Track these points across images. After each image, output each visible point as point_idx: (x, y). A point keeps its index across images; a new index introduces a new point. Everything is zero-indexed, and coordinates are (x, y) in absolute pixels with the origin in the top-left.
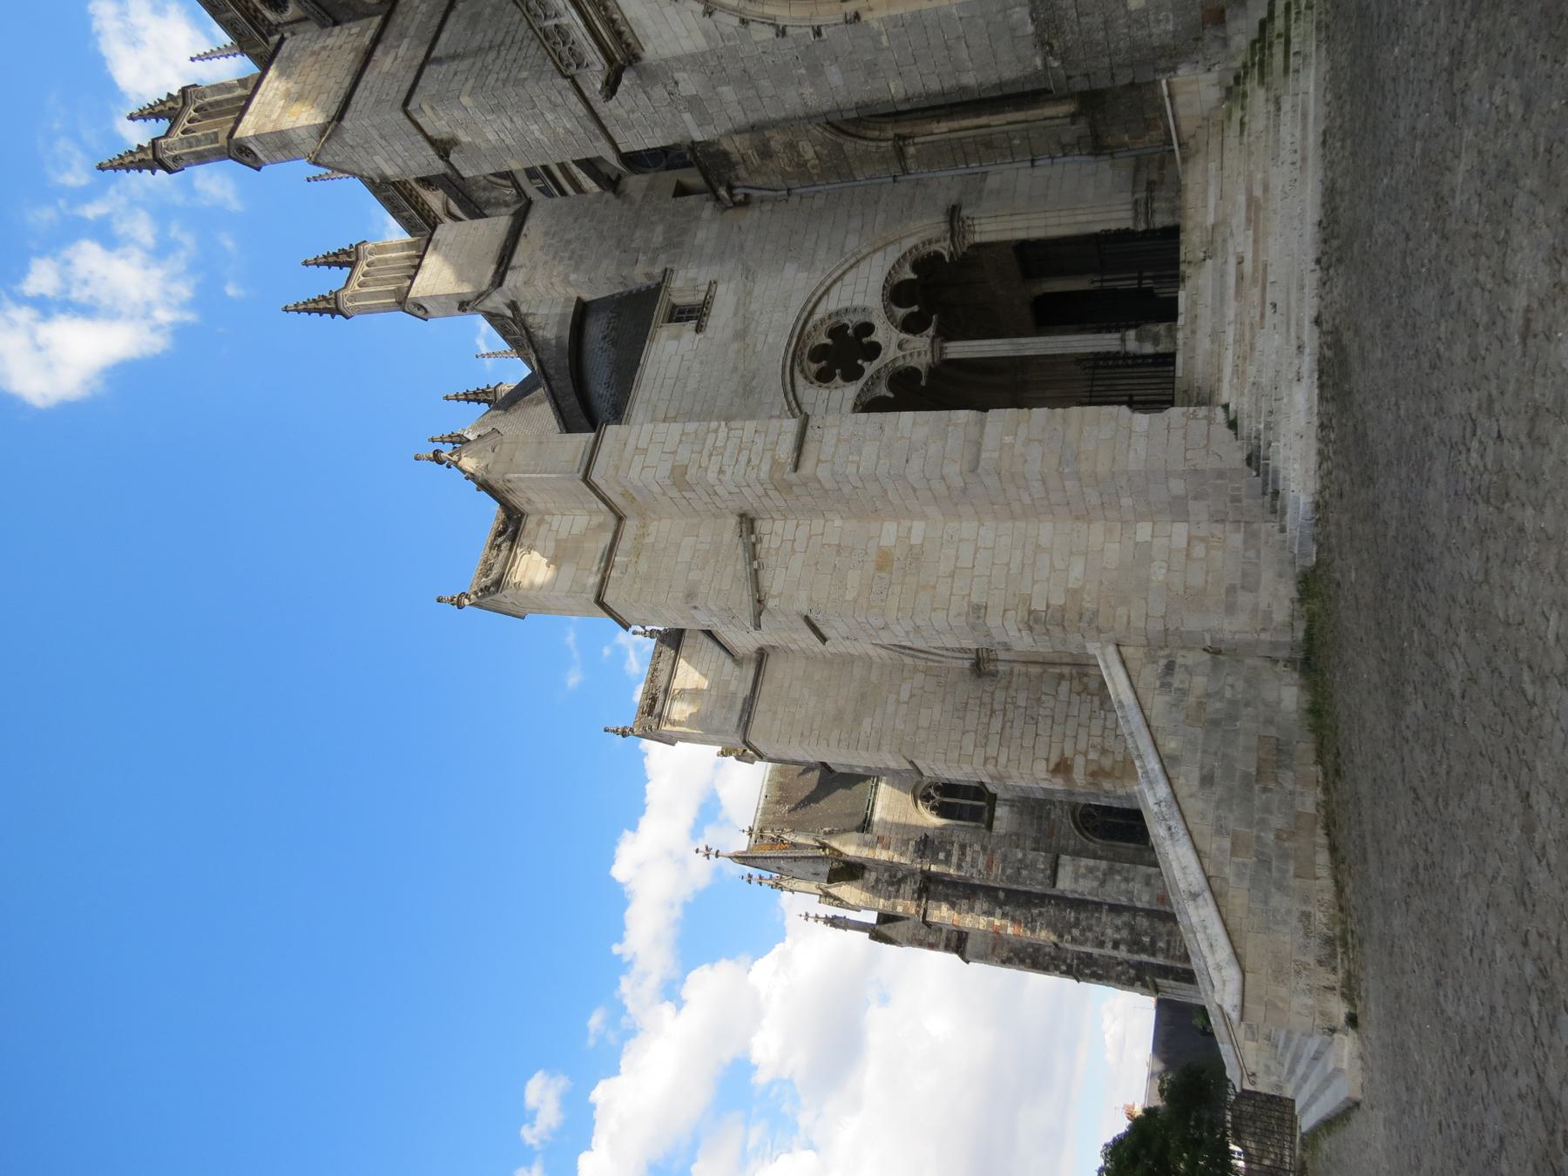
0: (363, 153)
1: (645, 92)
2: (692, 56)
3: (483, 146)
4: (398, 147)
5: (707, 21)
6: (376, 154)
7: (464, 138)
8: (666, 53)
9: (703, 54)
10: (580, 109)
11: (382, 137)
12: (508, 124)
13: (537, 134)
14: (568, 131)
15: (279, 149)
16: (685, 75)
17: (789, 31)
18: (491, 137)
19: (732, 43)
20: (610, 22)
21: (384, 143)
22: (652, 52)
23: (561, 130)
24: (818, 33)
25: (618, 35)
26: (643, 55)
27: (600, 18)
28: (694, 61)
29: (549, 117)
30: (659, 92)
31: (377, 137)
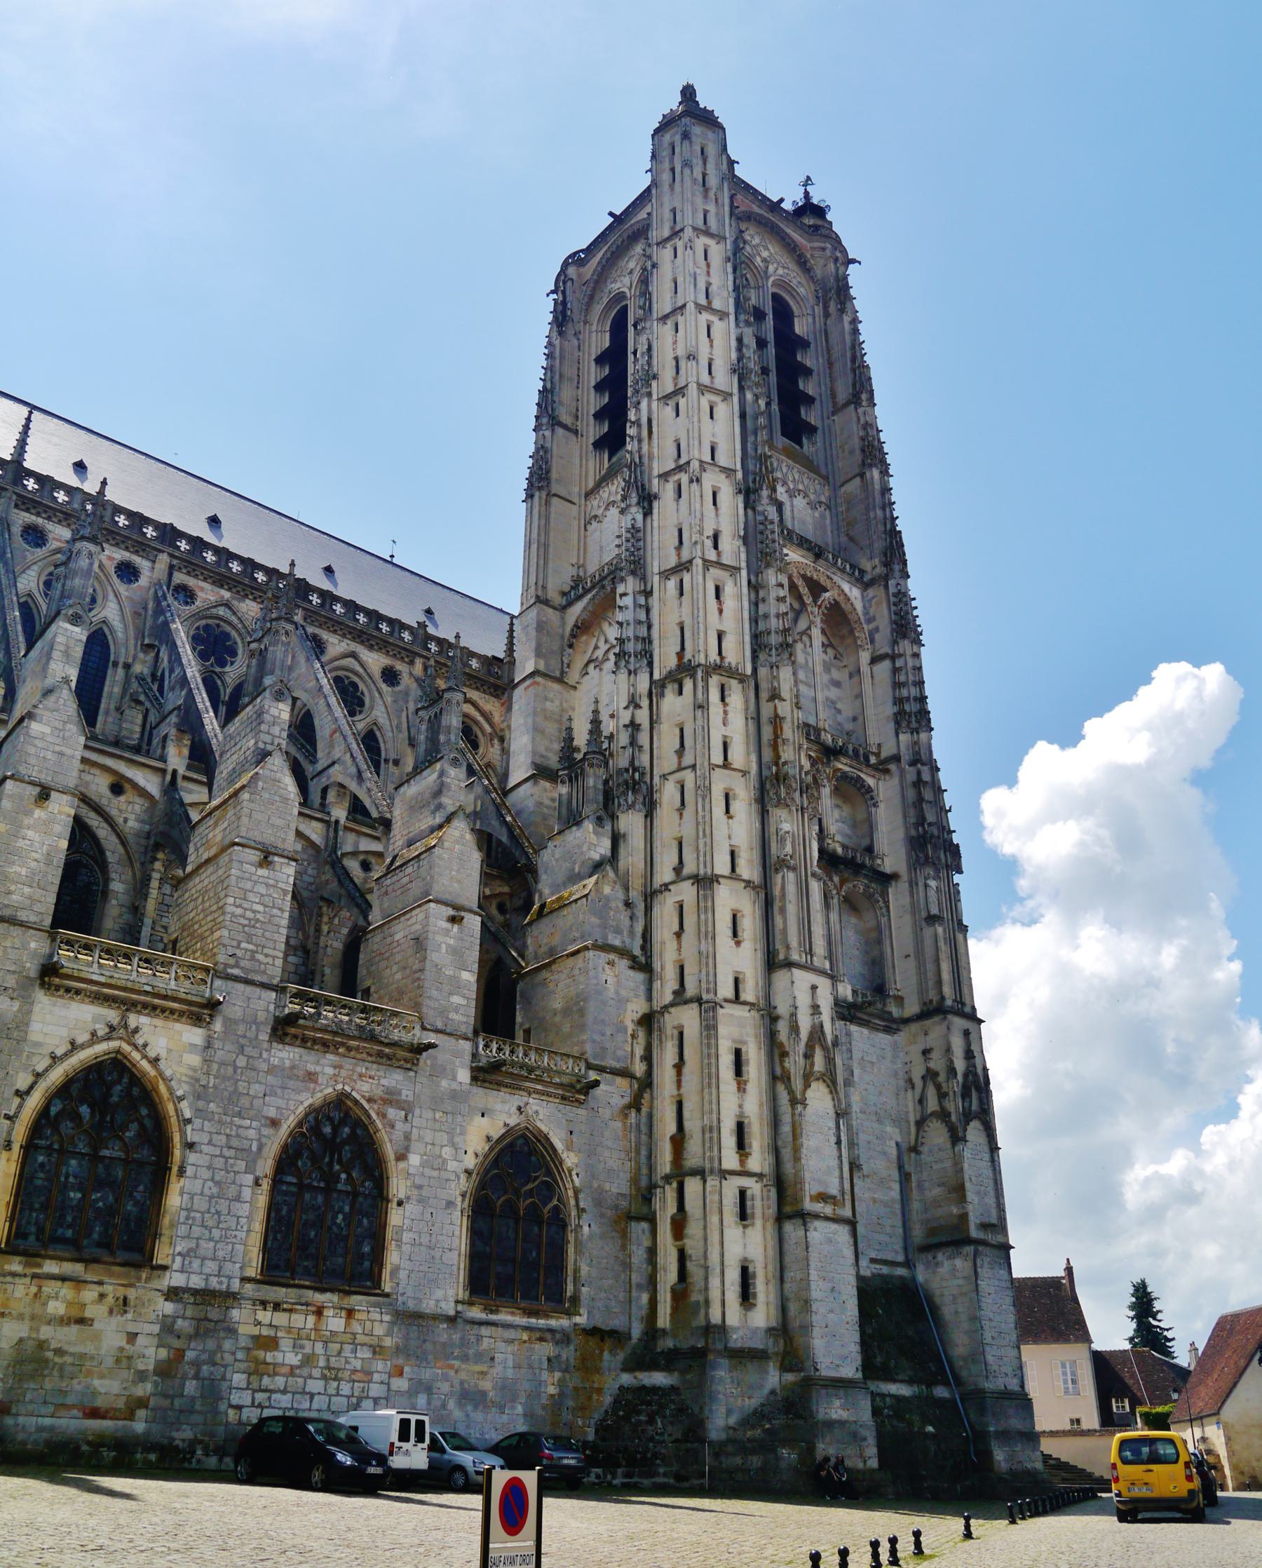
0: (57, 724)
1: (14, 972)
2: (27, 1024)
3: (26, 821)
4: (49, 755)
5: (47, 1051)
6: (52, 734)
7: (38, 813)
8: (37, 1008)
9: (26, 1033)
10: (23, 916)
11: (61, 754)
12: (35, 855)
13: (18, 869)
14: (9, 893)
15: (68, 647)
16: (15, 1009)
17: (17, 1100)
18: (30, 834)
19: (24, 1056)
20: (78, 992)
21: (57, 748)
22: (42, 1000)
23: (13, 888)
24: (7, 1117)
25: (68, 990)
26: (42, 992)
27: (85, 990)
28: (22, 1023)
29: (27, 890)
30: (11, 981)
31: (63, 749)
